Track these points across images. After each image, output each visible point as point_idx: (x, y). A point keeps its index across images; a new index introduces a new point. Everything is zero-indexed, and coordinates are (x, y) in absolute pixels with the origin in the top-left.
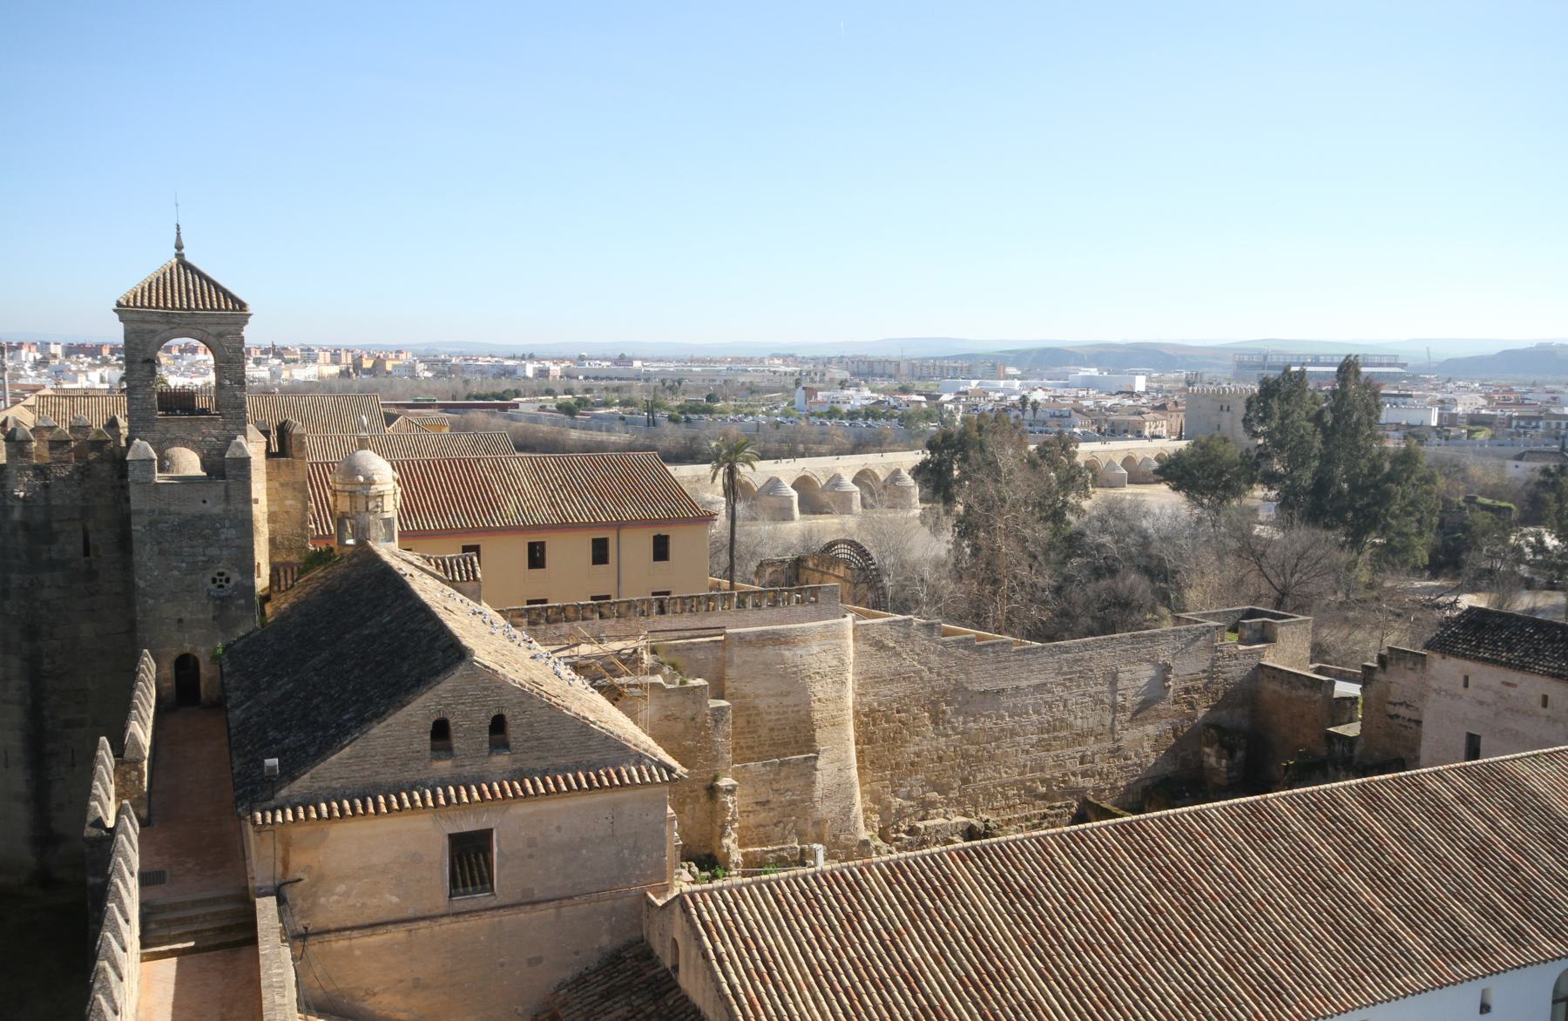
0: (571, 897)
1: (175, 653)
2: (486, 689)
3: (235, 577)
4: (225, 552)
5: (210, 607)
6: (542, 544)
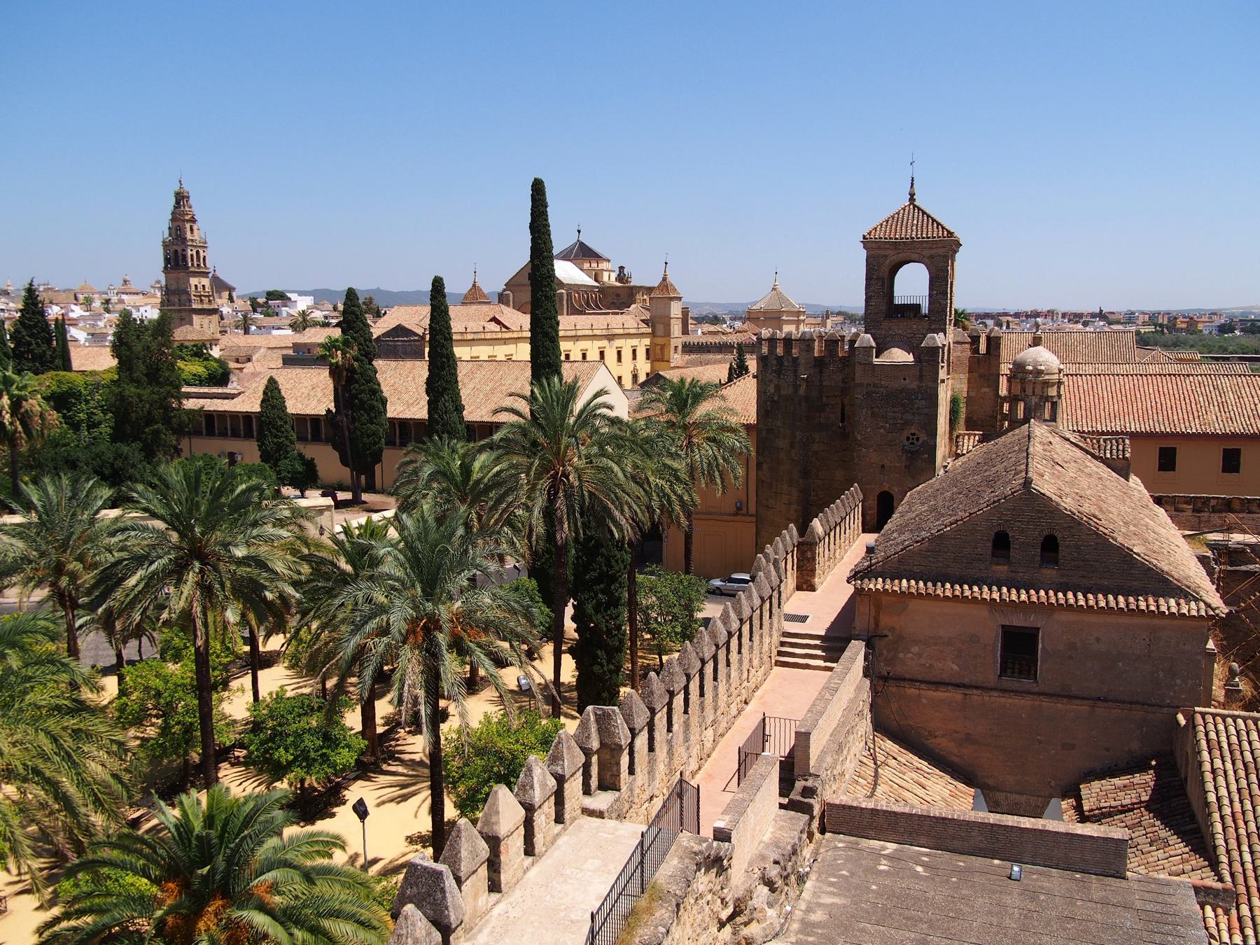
0: (1105, 700)
1: (878, 491)
2: (1040, 512)
3: (923, 437)
6: (1239, 451)
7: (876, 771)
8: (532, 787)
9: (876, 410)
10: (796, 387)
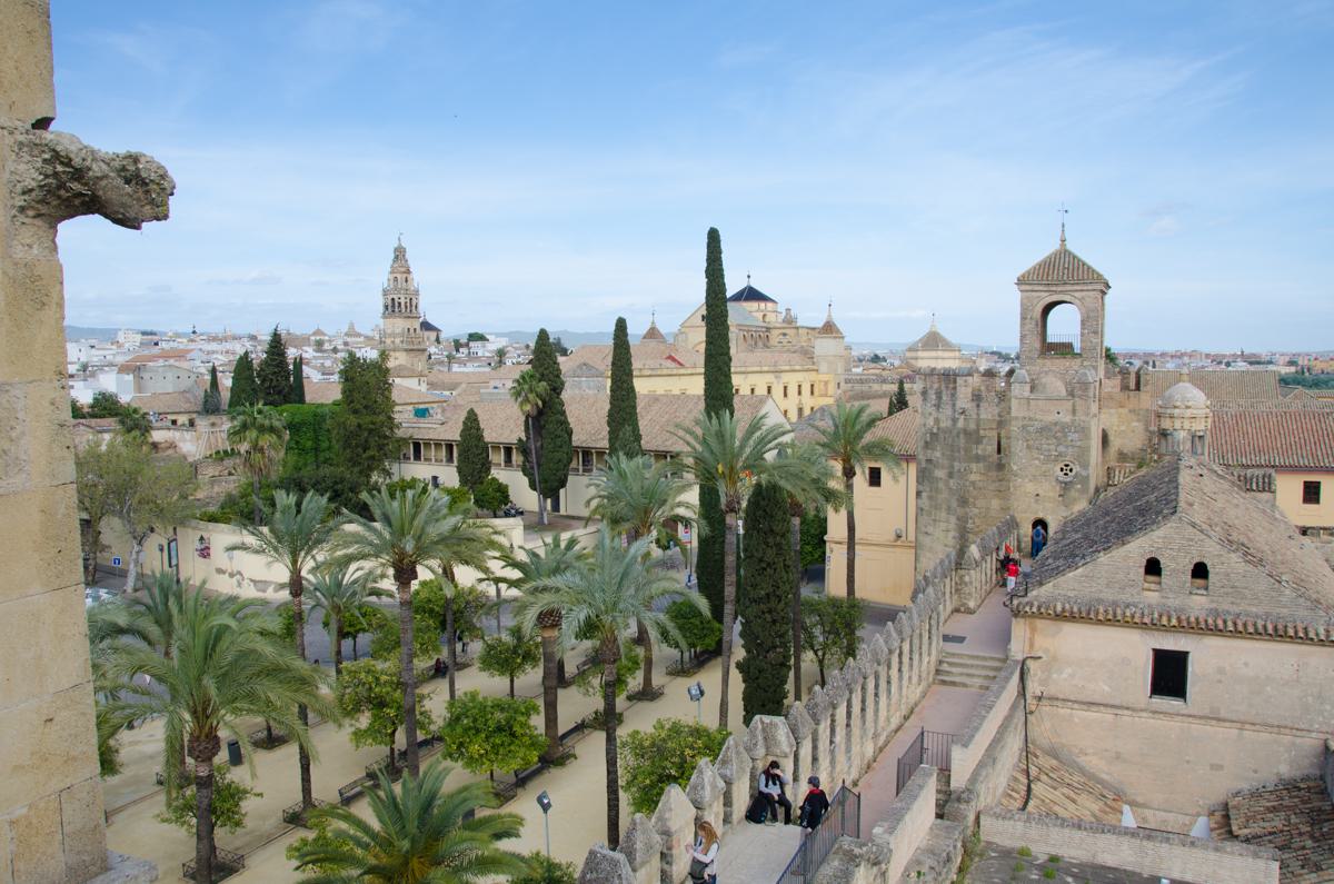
2: (1192, 540)
4: (1070, 450)
5: (1058, 488)
7: (1029, 790)
8: (703, 788)
9: (1031, 442)
10: (955, 421)
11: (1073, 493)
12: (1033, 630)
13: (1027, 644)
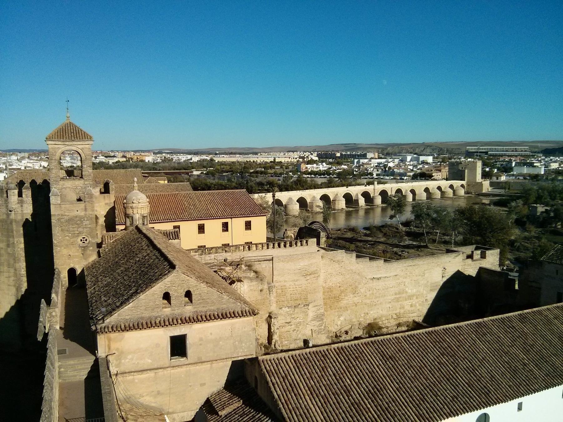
2: (183, 281)
5: (80, 250)
9: (63, 227)
11: (88, 252)
12: (109, 340)
13: (107, 347)
